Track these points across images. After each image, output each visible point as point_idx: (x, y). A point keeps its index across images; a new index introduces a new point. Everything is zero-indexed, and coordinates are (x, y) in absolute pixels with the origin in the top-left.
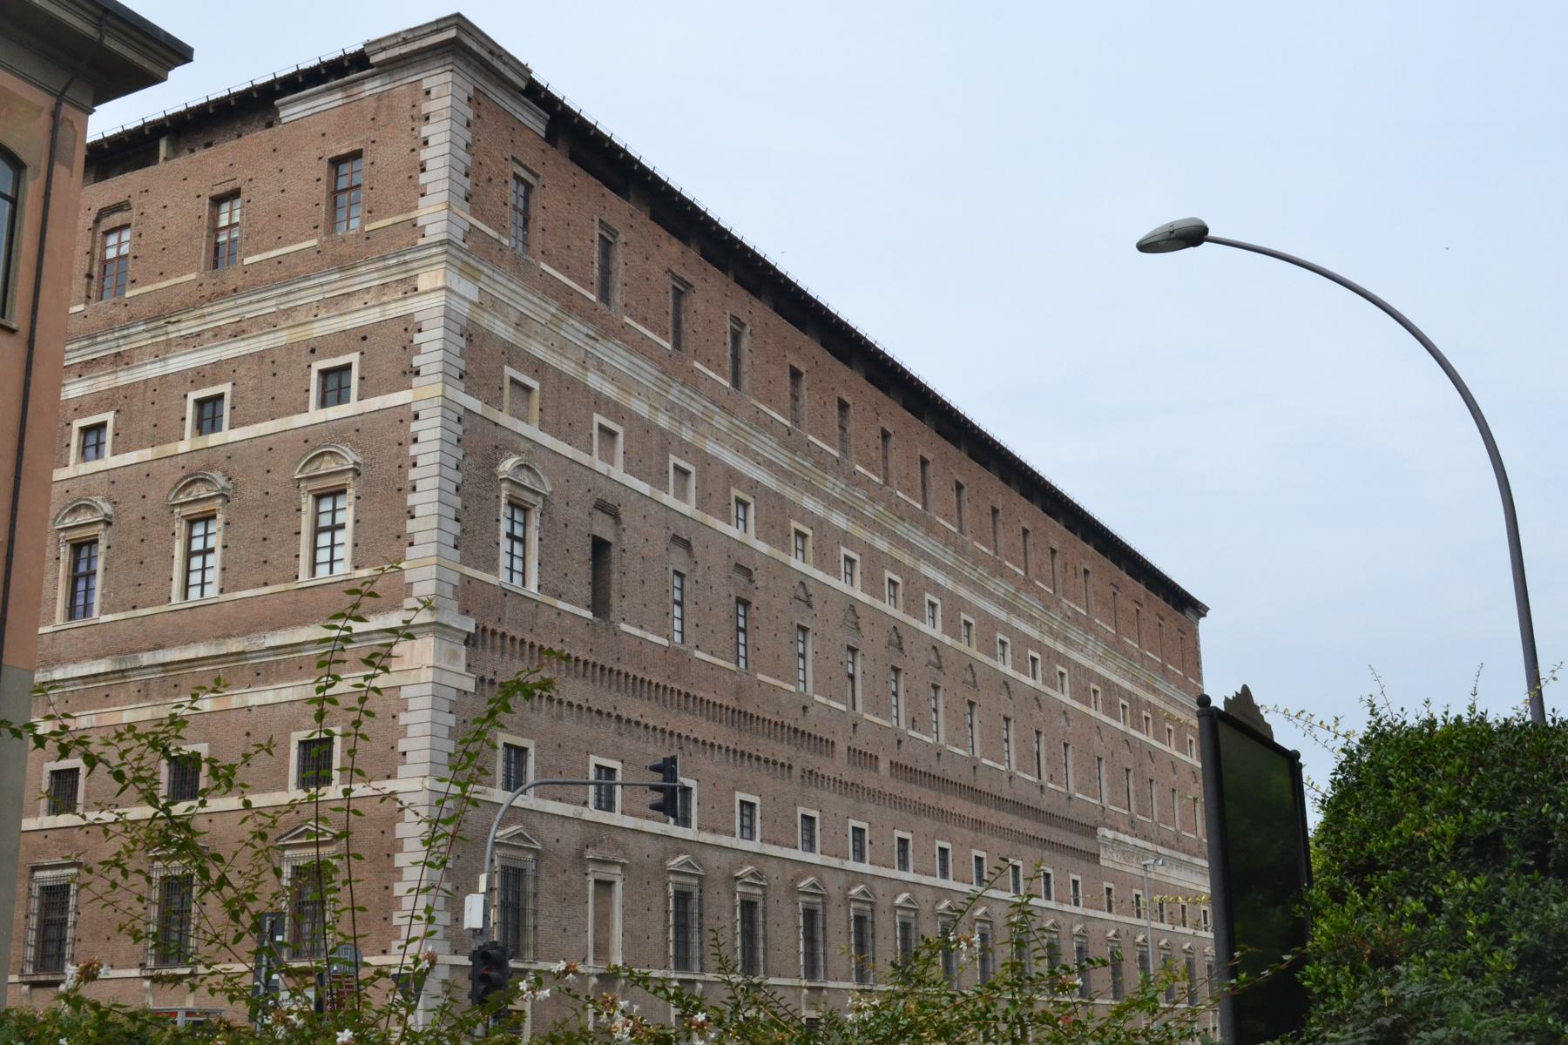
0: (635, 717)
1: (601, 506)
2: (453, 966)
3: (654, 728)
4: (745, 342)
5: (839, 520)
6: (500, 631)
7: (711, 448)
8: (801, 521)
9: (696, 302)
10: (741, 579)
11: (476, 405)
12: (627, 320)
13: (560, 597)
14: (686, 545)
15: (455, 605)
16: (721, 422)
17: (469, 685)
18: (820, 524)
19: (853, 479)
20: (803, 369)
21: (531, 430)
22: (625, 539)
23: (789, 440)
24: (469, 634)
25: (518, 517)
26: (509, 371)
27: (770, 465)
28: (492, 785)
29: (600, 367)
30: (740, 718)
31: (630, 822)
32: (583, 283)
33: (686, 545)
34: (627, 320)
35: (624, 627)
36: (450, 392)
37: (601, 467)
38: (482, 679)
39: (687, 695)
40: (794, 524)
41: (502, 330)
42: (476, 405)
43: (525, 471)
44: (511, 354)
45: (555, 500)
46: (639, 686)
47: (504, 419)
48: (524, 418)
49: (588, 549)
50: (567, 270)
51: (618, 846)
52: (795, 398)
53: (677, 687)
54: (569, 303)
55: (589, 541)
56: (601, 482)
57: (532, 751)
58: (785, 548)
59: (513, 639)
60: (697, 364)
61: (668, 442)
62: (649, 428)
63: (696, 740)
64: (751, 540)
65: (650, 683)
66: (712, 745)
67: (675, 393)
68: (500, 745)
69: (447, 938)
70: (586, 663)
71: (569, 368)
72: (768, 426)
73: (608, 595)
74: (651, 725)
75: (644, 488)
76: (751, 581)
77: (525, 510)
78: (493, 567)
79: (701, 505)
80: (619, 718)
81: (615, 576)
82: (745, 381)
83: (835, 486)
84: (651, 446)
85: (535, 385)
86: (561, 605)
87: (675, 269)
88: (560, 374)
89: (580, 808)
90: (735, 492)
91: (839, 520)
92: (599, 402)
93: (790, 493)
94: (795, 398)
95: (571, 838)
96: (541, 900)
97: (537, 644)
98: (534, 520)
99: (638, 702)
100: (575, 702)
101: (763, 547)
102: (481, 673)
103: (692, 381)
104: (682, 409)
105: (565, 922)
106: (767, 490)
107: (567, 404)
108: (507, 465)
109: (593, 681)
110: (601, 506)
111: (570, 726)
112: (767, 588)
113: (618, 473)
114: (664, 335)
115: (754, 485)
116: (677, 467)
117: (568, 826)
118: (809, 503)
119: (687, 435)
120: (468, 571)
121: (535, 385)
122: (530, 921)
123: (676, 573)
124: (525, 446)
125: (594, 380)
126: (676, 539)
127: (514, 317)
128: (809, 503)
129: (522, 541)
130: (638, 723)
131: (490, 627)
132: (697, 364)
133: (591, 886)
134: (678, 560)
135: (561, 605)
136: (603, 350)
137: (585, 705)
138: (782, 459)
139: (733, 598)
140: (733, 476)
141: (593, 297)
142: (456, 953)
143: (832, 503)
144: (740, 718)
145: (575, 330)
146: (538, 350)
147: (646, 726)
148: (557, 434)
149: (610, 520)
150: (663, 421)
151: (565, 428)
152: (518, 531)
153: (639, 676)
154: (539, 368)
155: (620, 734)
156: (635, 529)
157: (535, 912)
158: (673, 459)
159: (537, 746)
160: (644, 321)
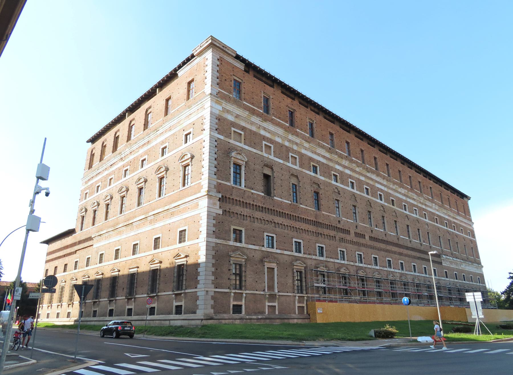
0: (280, 222)
1: (266, 165)
2: (215, 292)
3: (287, 226)
4: (314, 125)
5: (348, 172)
6: (231, 198)
7: (303, 151)
8: (335, 172)
9: (297, 115)
10: (316, 186)
11: (222, 137)
12: (273, 117)
13: (252, 189)
14: (297, 177)
15: (215, 190)
16: (306, 145)
17: (220, 212)
18: (341, 173)
19: (351, 161)
20: (333, 133)
21: (242, 145)
22: (275, 174)
23: (329, 150)
24: (220, 198)
25: (238, 167)
26: (233, 129)
27: (324, 157)
28: (229, 240)
29: (265, 129)
30: (316, 223)
31: (279, 251)
32: (258, 107)
33: (297, 177)
34: (273, 117)
35: (275, 198)
36: (212, 133)
37: (266, 155)
38: (225, 211)
39: (298, 217)
40: (333, 172)
41: (230, 118)
42: (222, 137)
43: (239, 155)
44: (233, 124)
45: (250, 163)
46: (281, 214)
47: (232, 141)
48: (241, 142)
49: (262, 177)
50: (253, 104)
51: (275, 258)
52: (332, 140)
53: (294, 215)
54: (253, 112)
55: (262, 175)
56: (266, 159)
57: (243, 231)
58: (331, 179)
59: (236, 200)
60: (298, 130)
61: (288, 150)
62: (282, 146)
63: (302, 229)
64: (318, 176)
65: (285, 213)
66: (308, 231)
67: (290, 137)
68: (232, 229)
69: (213, 283)
70: (262, 207)
71: (254, 129)
72: (323, 147)
73: (271, 190)
74: (286, 225)
75: (281, 161)
76: (319, 187)
77: (240, 166)
78: (229, 180)
79: (301, 166)
80: (275, 222)
81: (272, 185)
82: (315, 135)
83: (346, 163)
84: (283, 151)
85: (243, 133)
86: (252, 191)
87: (289, 105)
88: (251, 130)
89: (261, 247)
90: (312, 163)
91: (348, 172)
92: (264, 138)
93: (331, 164)
94: (332, 140)
95: (258, 256)
96: (247, 273)
97: (245, 201)
98: (243, 168)
99: (281, 218)
100: (259, 218)
101: (322, 178)
102: (224, 209)
103: (297, 135)
104: (293, 142)
105: (257, 279)
106: (323, 163)
107: (253, 138)
108: (233, 154)
109: (266, 213)
110: (266, 165)
111: (257, 225)
112: (324, 189)
113: (272, 157)
114: (287, 122)
115: (318, 162)
116: (291, 156)
117: (257, 252)
118: (338, 167)
119: (295, 147)
120: (219, 181)
121: (243, 133)
122: (243, 279)
123: (293, 184)
124: (239, 149)
125: (262, 132)
126: (292, 175)
127: (235, 115)
128: (338, 167)
129: (240, 174)
130: (281, 224)
131: (228, 196)
132: (298, 130)
133: (266, 269)
134: (294, 181)
135: (252, 191)
136: (265, 125)
137: (262, 219)
138: (327, 155)
139: (313, 191)
140: (311, 159)
141: (262, 111)
142: (216, 288)
143: (345, 167)
144: (316, 223)
145: (256, 119)
146: (243, 124)
147: (284, 225)
148: (250, 146)
149: (270, 170)
150: (287, 144)
151: (253, 144)
152: (238, 171)
153: (281, 211)
154: (243, 129)
155: (276, 227)
156: (278, 172)
157: (245, 276)
158: (290, 154)
159: (245, 230)
160: (279, 118)
